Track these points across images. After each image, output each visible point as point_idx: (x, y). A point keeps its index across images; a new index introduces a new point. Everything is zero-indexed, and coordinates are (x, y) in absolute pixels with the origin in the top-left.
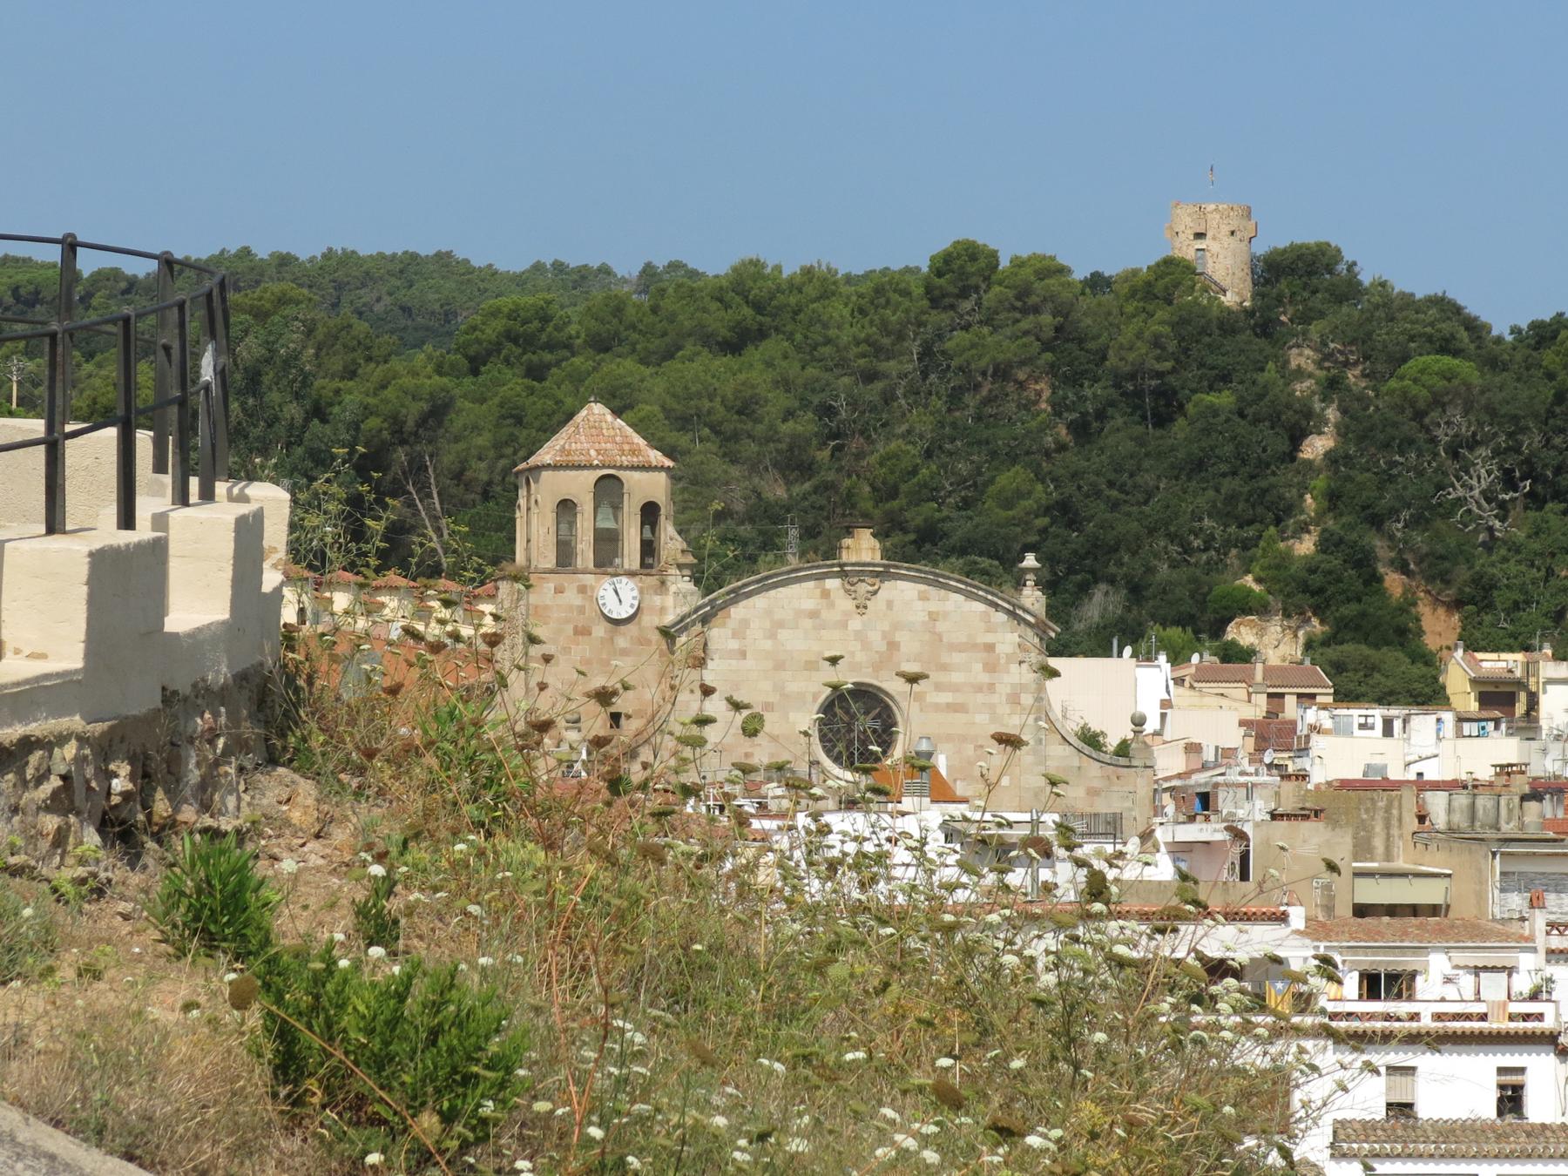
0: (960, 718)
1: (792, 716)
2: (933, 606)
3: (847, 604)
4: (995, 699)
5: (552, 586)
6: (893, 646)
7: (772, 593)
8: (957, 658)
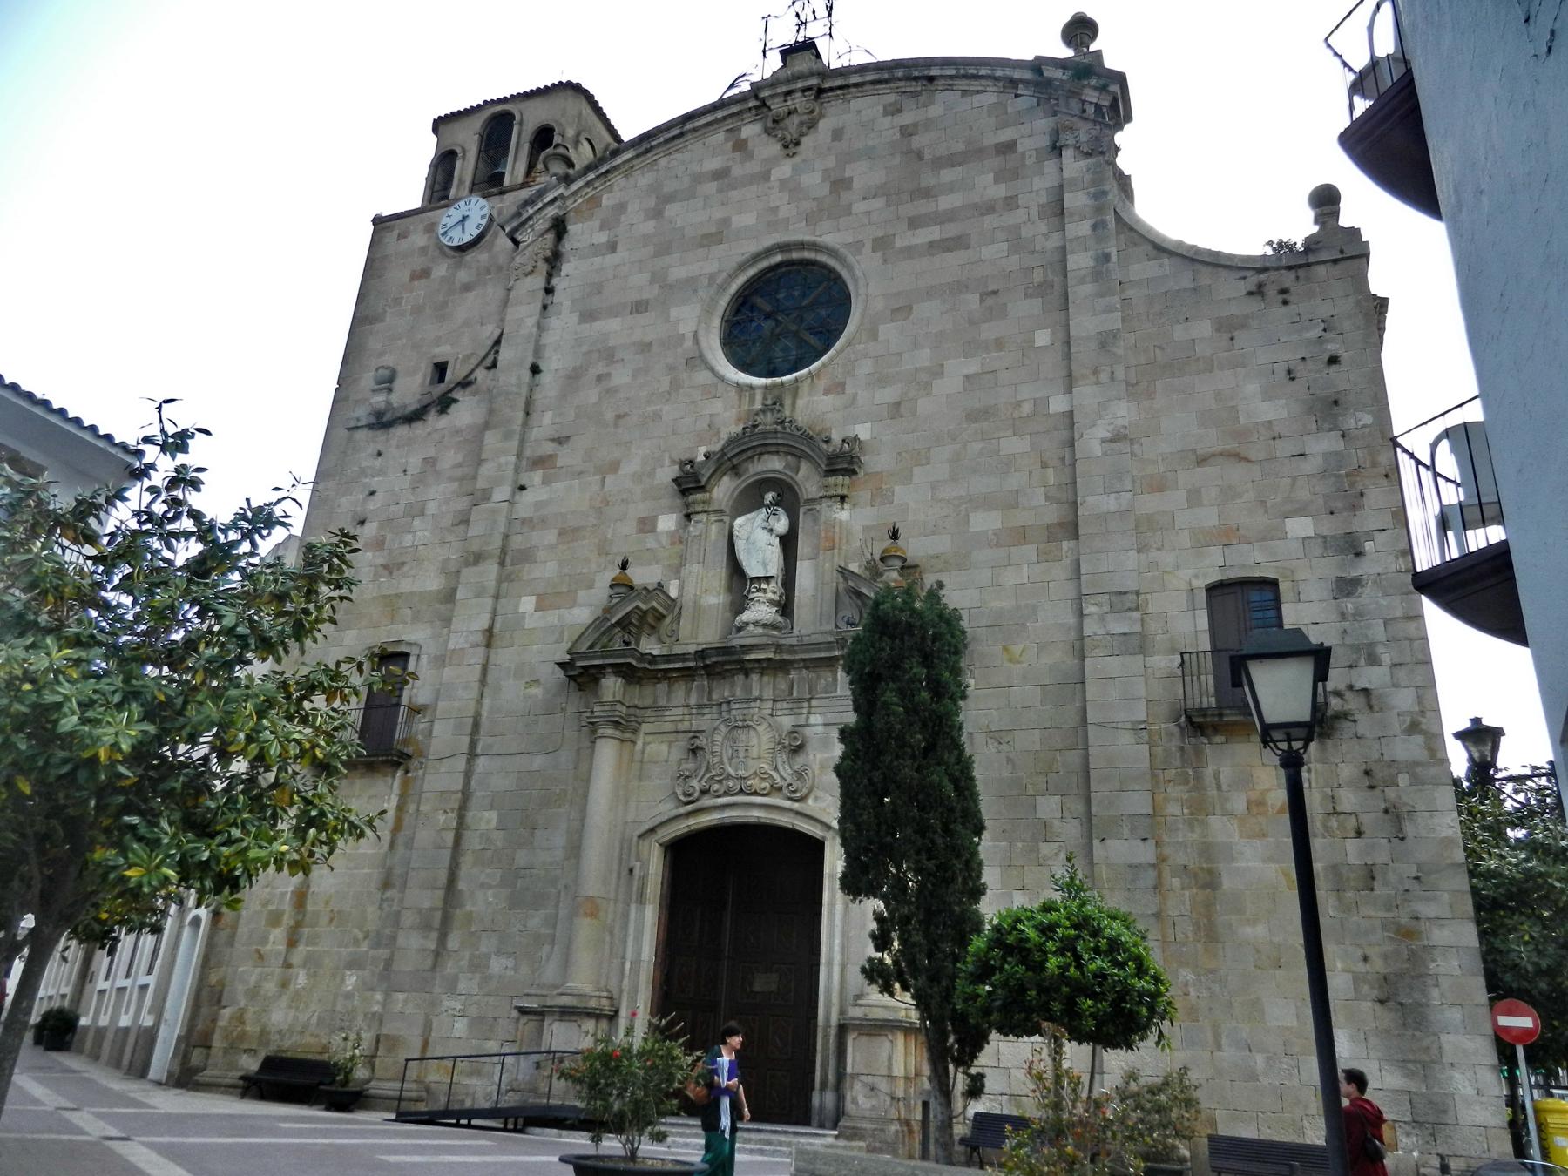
0: (953, 259)
1: (674, 312)
2: (907, 118)
3: (775, 148)
4: (1019, 216)
5: (396, 232)
8: (948, 175)
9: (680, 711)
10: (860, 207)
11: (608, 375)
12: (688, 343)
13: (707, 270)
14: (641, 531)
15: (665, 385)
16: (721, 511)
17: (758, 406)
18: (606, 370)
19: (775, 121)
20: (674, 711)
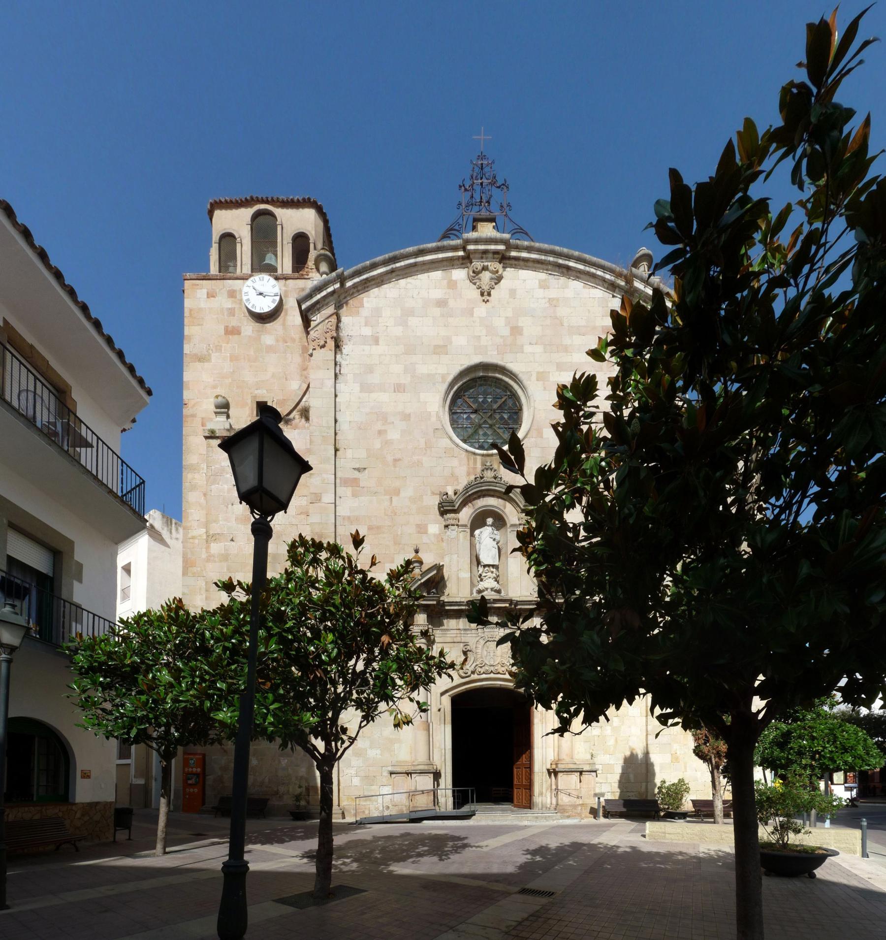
2: (553, 293)
5: (205, 291)
6: (516, 331)
7: (402, 282)
9: (455, 632)
10: (528, 349)
11: (385, 431)
12: (434, 419)
13: (440, 371)
14: (419, 532)
15: (422, 441)
16: (465, 526)
17: (479, 466)
18: (383, 428)
19: (474, 272)
20: (452, 632)
